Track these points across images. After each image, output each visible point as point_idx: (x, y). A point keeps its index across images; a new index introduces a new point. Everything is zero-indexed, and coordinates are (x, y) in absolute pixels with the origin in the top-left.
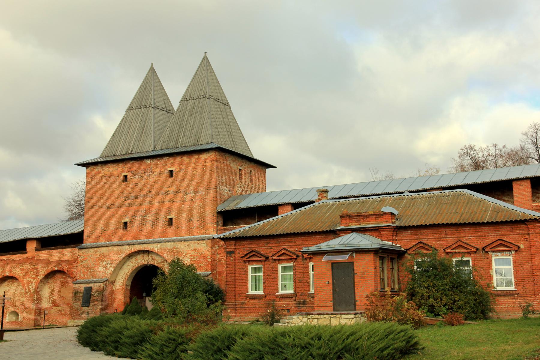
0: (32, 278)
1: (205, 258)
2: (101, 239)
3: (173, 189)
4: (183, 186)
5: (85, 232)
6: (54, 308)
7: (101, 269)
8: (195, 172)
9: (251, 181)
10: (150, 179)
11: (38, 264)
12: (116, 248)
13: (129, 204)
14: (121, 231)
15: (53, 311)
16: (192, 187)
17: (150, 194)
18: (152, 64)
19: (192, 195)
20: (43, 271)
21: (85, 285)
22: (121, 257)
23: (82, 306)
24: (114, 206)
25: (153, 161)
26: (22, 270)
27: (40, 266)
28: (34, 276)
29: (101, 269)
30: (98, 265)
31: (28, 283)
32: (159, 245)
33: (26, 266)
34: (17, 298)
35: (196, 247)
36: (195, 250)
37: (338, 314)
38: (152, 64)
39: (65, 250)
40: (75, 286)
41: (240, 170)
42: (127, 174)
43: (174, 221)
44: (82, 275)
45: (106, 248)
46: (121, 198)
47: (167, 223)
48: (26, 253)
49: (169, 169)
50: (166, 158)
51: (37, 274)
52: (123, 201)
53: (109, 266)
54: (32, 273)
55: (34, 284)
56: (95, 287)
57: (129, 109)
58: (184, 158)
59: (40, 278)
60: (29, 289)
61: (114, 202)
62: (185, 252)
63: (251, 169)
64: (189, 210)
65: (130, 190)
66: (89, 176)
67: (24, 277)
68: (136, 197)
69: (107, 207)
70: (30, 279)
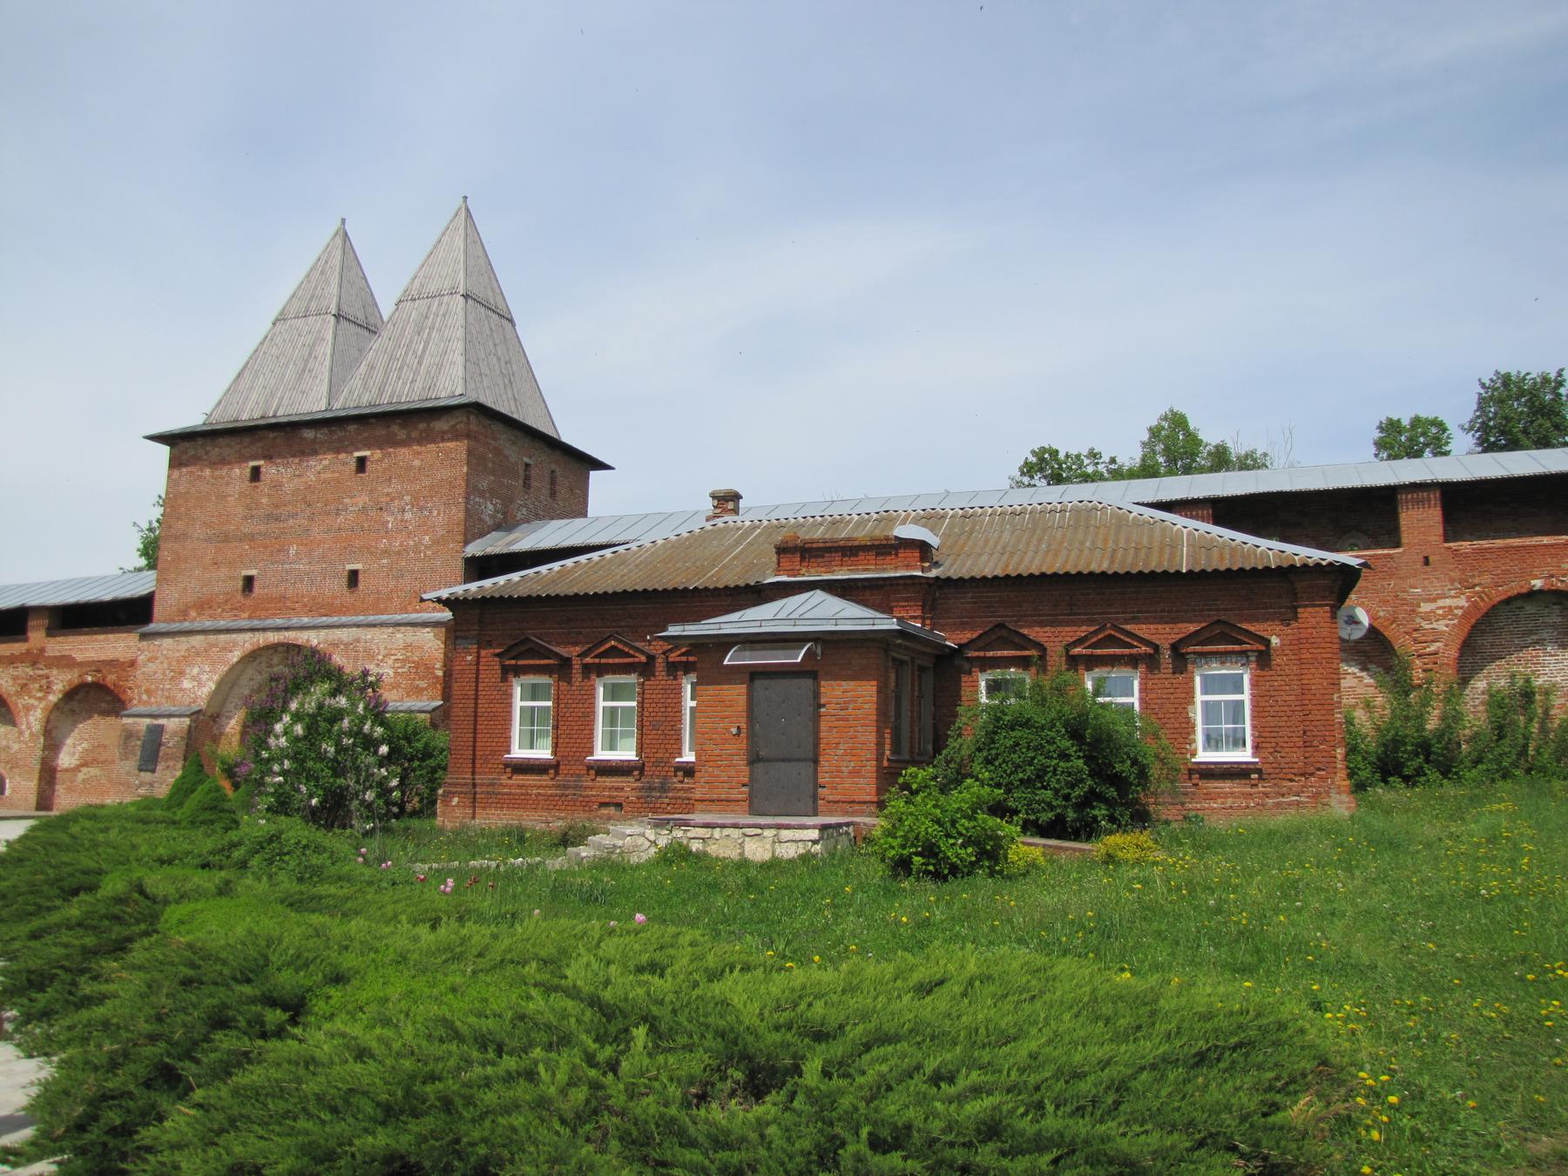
1: (429, 669)
2: (193, 614)
3: (363, 499)
4: (388, 494)
5: (157, 597)
6: (84, 770)
7: (187, 684)
8: (417, 463)
9: (553, 494)
10: (311, 477)
11: (49, 666)
12: (222, 637)
13: (260, 534)
14: (239, 596)
15: (80, 776)
16: (407, 498)
17: (308, 513)
18: (343, 221)
19: (408, 516)
20: (61, 681)
21: (148, 721)
22: (235, 656)
23: (141, 770)
24: (226, 539)
25: (321, 434)
26: (15, 678)
28: (40, 694)
29: (187, 684)
30: (182, 673)
31: (28, 709)
32: (323, 633)
33: (25, 670)
35: (409, 641)
36: (407, 647)
37: (770, 827)
38: (343, 221)
39: (111, 636)
40: (126, 721)
41: (527, 465)
43: (361, 577)
44: (144, 697)
45: (200, 638)
46: (245, 518)
47: (345, 581)
48: (26, 640)
49: (357, 454)
50: (352, 428)
51: (48, 689)
53: (204, 677)
56: (171, 724)
57: (280, 319)
58: (395, 428)
59: (53, 698)
62: (383, 652)
63: (553, 467)
64: (398, 553)
65: (265, 500)
66: (175, 463)
67: (18, 694)
68: (277, 519)
69: (208, 540)
70: (32, 701)
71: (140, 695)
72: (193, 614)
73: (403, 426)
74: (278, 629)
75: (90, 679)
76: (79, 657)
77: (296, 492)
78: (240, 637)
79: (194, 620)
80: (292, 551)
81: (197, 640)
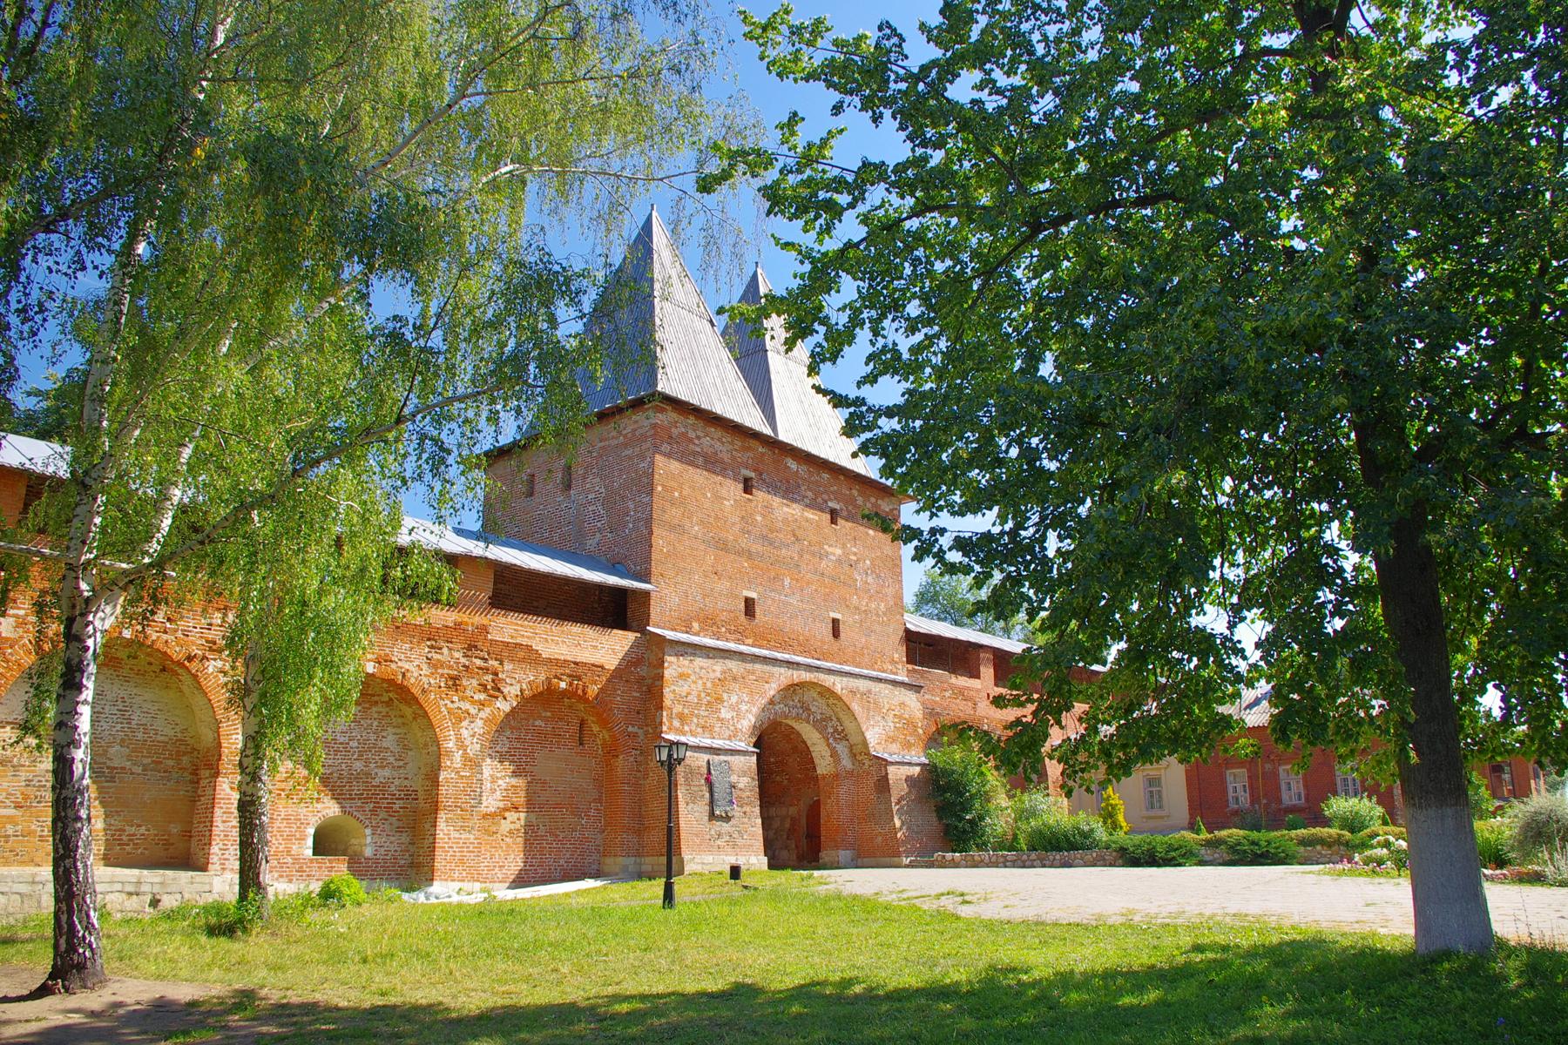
0: (473, 702)
14: (742, 617)
20: (518, 682)
22: (772, 690)
24: (722, 546)
27: (508, 666)
28: (482, 696)
29: (725, 713)
30: (719, 700)
31: (459, 717)
33: (452, 655)
34: (358, 765)
42: (753, 475)
44: (676, 723)
51: (496, 690)
52: (744, 542)
54: (475, 682)
55: (480, 723)
59: (504, 706)
60: (459, 739)
61: (723, 535)
65: (759, 518)
70: (466, 706)
71: (670, 718)
72: (696, 625)
73: (861, 493)
74: (809, 668)
75: (563, 685)
76: (547, 650)
77: (785, 521)
78: (777, 670)
79: (697, 634)
80: (787, 581)
81: (734, 665)
